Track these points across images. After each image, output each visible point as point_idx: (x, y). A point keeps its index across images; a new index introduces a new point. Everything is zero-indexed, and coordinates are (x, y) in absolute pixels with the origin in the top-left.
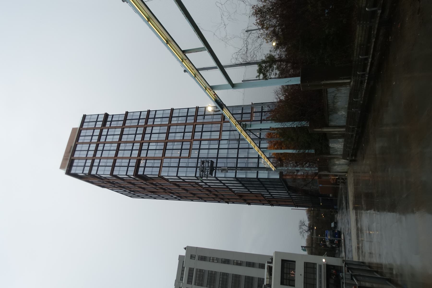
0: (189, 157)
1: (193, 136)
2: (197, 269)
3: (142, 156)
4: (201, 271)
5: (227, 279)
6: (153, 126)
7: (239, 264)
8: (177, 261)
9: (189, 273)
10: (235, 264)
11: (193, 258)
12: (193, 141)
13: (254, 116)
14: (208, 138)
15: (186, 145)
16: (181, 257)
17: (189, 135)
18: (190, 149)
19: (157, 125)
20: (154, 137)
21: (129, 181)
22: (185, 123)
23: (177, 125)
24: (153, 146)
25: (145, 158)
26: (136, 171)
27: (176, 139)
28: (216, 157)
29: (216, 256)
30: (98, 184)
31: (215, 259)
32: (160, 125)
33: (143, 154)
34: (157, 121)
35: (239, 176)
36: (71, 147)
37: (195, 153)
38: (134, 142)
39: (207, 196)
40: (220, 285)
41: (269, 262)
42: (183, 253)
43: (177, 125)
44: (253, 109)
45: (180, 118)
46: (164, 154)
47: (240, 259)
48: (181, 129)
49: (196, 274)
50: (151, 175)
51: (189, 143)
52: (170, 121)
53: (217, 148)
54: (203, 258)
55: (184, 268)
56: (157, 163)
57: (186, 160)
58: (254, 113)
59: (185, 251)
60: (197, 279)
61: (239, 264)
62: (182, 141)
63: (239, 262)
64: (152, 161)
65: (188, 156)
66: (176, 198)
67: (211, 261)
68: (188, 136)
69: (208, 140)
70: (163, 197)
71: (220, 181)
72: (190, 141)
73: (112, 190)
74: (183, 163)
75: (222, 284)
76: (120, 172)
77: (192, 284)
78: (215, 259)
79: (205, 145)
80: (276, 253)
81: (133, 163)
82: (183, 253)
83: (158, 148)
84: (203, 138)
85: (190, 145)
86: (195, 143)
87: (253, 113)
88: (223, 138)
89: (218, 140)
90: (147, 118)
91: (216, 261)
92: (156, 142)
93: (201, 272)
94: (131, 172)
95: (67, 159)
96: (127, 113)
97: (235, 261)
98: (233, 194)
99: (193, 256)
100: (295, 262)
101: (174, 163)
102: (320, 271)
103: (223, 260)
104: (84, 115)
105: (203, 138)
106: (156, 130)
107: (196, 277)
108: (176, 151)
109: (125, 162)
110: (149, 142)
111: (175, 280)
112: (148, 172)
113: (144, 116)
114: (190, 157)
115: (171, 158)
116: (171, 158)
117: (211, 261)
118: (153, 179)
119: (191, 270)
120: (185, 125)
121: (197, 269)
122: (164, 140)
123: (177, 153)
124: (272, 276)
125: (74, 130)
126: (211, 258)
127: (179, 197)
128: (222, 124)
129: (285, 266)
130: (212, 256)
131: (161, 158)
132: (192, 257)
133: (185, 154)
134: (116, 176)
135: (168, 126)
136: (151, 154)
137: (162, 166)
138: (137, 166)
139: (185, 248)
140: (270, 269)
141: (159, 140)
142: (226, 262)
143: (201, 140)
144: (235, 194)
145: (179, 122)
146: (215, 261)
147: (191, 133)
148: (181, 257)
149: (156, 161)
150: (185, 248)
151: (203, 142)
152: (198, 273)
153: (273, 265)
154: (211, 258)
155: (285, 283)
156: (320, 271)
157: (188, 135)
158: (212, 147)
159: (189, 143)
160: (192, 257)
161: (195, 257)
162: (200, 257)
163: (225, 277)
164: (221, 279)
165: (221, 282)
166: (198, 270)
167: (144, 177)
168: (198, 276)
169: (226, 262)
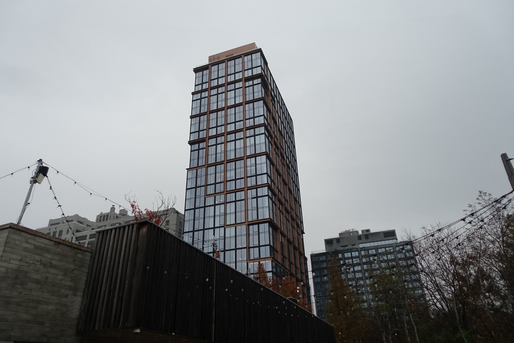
0: (207, 195)
11: (167, 223)
13: (254, 263)
15: (220, 188)
36: (232, 54)
44: (263, 260)
57: (203, 194)
58: (258, 262)
83: (217, 155)
86: (223, 196)
87: (258, 260)
88: (228, 230)
95: (214, 60)
104: (261, 49)
114: (206, 196)
125: (253, 44)
128: (246, 224)
136: (212, 150)
158: (217, 219)
161: (168, 225)
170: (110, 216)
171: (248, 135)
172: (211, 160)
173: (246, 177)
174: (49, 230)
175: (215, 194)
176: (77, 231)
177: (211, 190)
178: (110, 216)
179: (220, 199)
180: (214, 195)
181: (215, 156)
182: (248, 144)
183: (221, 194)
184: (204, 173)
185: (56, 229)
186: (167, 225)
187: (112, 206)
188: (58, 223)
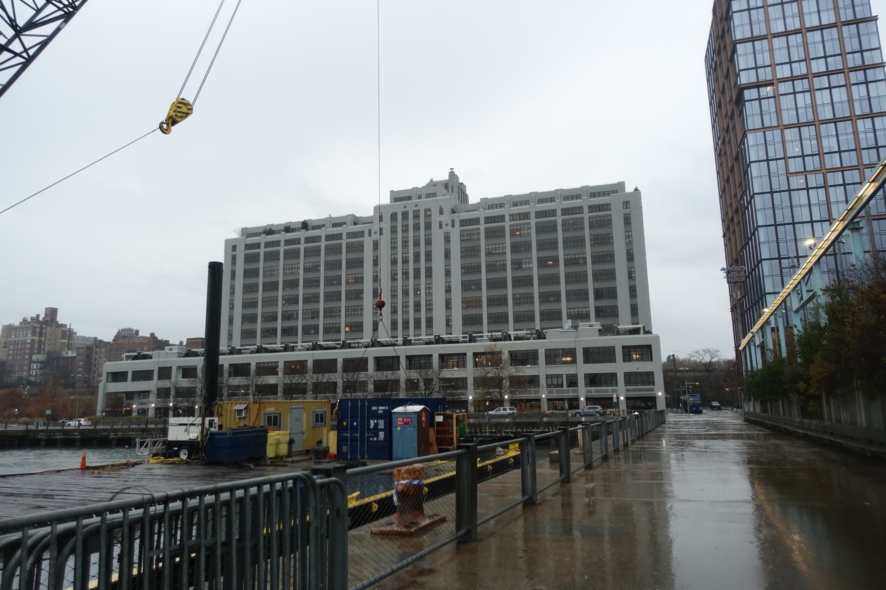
0: (788, 174)
1: (833, 170)
2: (610, 215)
3: (781, 85)
4: (609, 222)
5: (607, 261)
6: (848, 86)
7: (631, 276)
8: (615, 182)
9: (603, 205)
10: (630, 270)
11: (625, 205)
12: (823, 174)
14: (832, 199)
15: (812, 163)
16: (622, 185)
17: (835, 162)
18: (805, 172)
19: (850, 94)
20: (823, 97)
21: (731, 71)
22: (860, 148)
23: (856, 133)
24: (803, 100)
25: (776, 93)
26: (750, 87)
27: (823, 140)
28: (795, 222)
29: (634, 239)
30: (717, 6)
31: (630, 239)
32: (851, 101)
33: (784, 88)
34: (859, 92)
35: (766, 267)
37: (798, 182)
38: (807, 60)
39: (733, 195)
40: (597, 254)
41: (644, 327)
42: (629, 189)
43: (856, 133)
45: (872, 135)
46: (790, 126)
47: (637, 275)
48: (848, 142)
49: (604, 216)
50: (746, 116)
51: (818, 166)
52: (863, 117)
53: (814, 220)
54: (627, 220)
55: (608, 195)
56: (770, 120)
57: (782, 170)
59: (632, 190)
60: (598, 219)
61: (631, 276)
62: (820, 154)
63: (633, 275)
64: (773, 109)
65: (790, 172)
66: (717, 144)
67: (627, 234)
68: (833, 161)
69: (827, 200)
70: (715, 121)
71: (754, 234)
72: (823, 168)
73: (710, 35)
74: (777, 167)
75: (599, 256)
76: (744, 57)
77: (589, 212)
78: (630, 239)
79: (818, 196)
80: (658, 337)
81: (765, 75)
82: (629, 189)
84: (831, 190)
85: (813, 169)
86: (820, 176)
89: (829, 217)
90: (864, 68)
91: (628, 241)
92: (812, 103)
93: (607, 222)
94: (745, 78)
96: (875, 19)
97: (633, 269)
98: (739, 249)
99: (628, 204)
100: (652, 360)
101: (775, 151)
102: (646, 390)
103: (631, 251)
105: (831, 190)
106: (840, 95)
107: (600, 217)
108: (800, 145)
109: (764, 58)
110: (811, 91)
111: (588, 186)
112: (751, 109)
113: (869, 58)
115: (783, 142)
116: (783, 142)
117: (627, 234)
118: (740, 116)
119: (606, 207)
120: (858, 150)
121: (610, 215)
122: (818, 118)
123: (794, 149)
124: (629, 334)
126: (630, 233)
127: (720, 150)
129: (644, 349)
130: (634, 233)
131: (780, 124)
132: (626, 204)
133: (795, 165)
134: (734, 50)
135: (851, 117)
136: (786, 102)
137: (765, 130)
138: (758, 85)
139: (636, 189)
140: (636, 331)
141: (818, 108)
142: (630, 257)
143: (825, 187)
144: (739, 254)
145: (862, 136)
146: (627, 239)
147: (839, 166)
148: (622, 185)
149: (774, 116)
150: (636, 189)
151: (822, 191)
152: (606, 218)
153: (642, 335)
154: (630, 233)
155: (625, 350)
156: (646, 390)
157: (834, 161)
158: (815, 210)
159: (818, 166)
160: (626, 204)
161: (627, 208)
162: (629, 216)
163: (609, 259)
164: (605, 253)
165: (600, 254)
166: (609, 218)
167: (740, 101)
168: (602, 219)
169: (630, 257)
170: (452, 186)
171: (853, 81)
172: (788, 118)
173: (858, 150)
174: (405, 207)
175: (805, 172)
176: (453, 212)
177: (795, 165)
178: (452, 186)
179: (813, 181)
180: (805, 174)
181: (795, 112)
182: (855, 96)
183: (816, 172)
184: (778, 138)
185: (416, 206)
186: (625, 207)
187: (450, 171)
188: (409, 198)
